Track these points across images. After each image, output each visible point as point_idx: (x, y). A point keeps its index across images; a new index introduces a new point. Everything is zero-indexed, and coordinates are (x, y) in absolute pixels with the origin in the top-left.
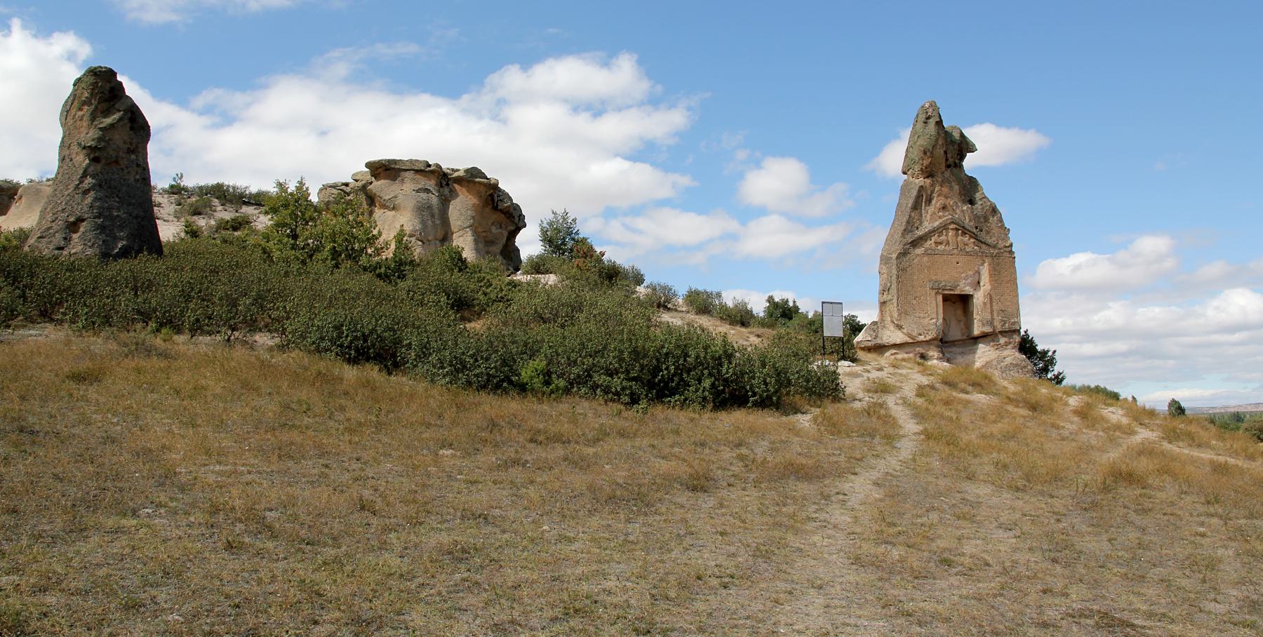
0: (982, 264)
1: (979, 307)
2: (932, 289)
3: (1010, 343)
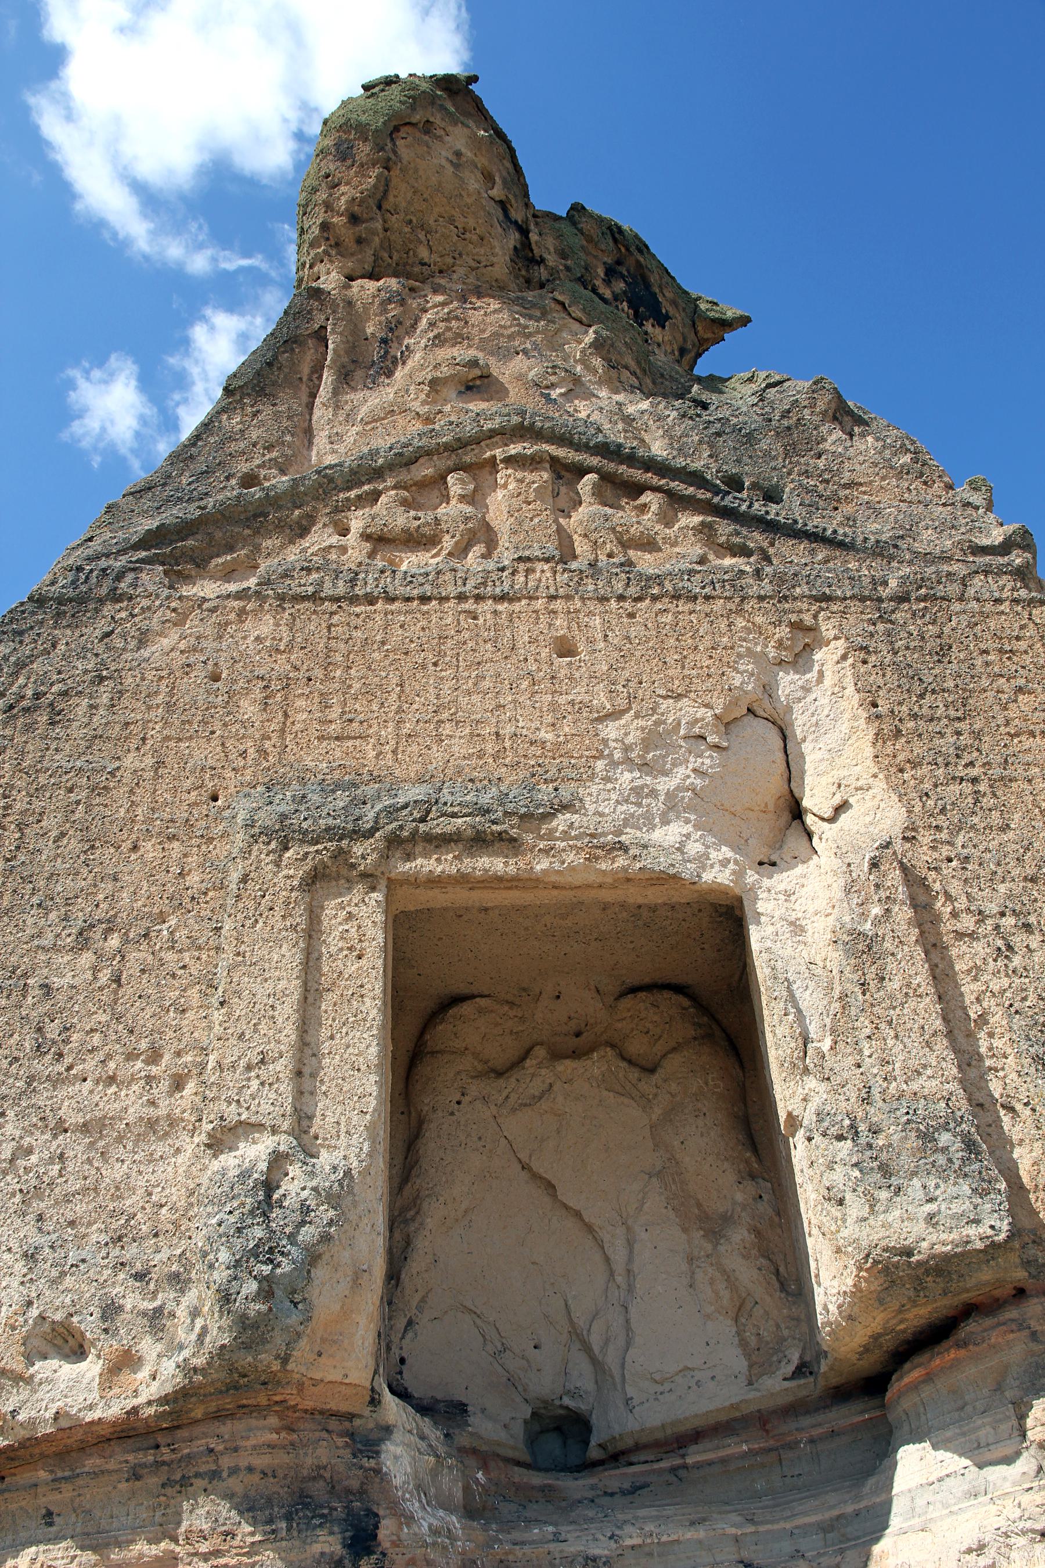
1: (810, 999)
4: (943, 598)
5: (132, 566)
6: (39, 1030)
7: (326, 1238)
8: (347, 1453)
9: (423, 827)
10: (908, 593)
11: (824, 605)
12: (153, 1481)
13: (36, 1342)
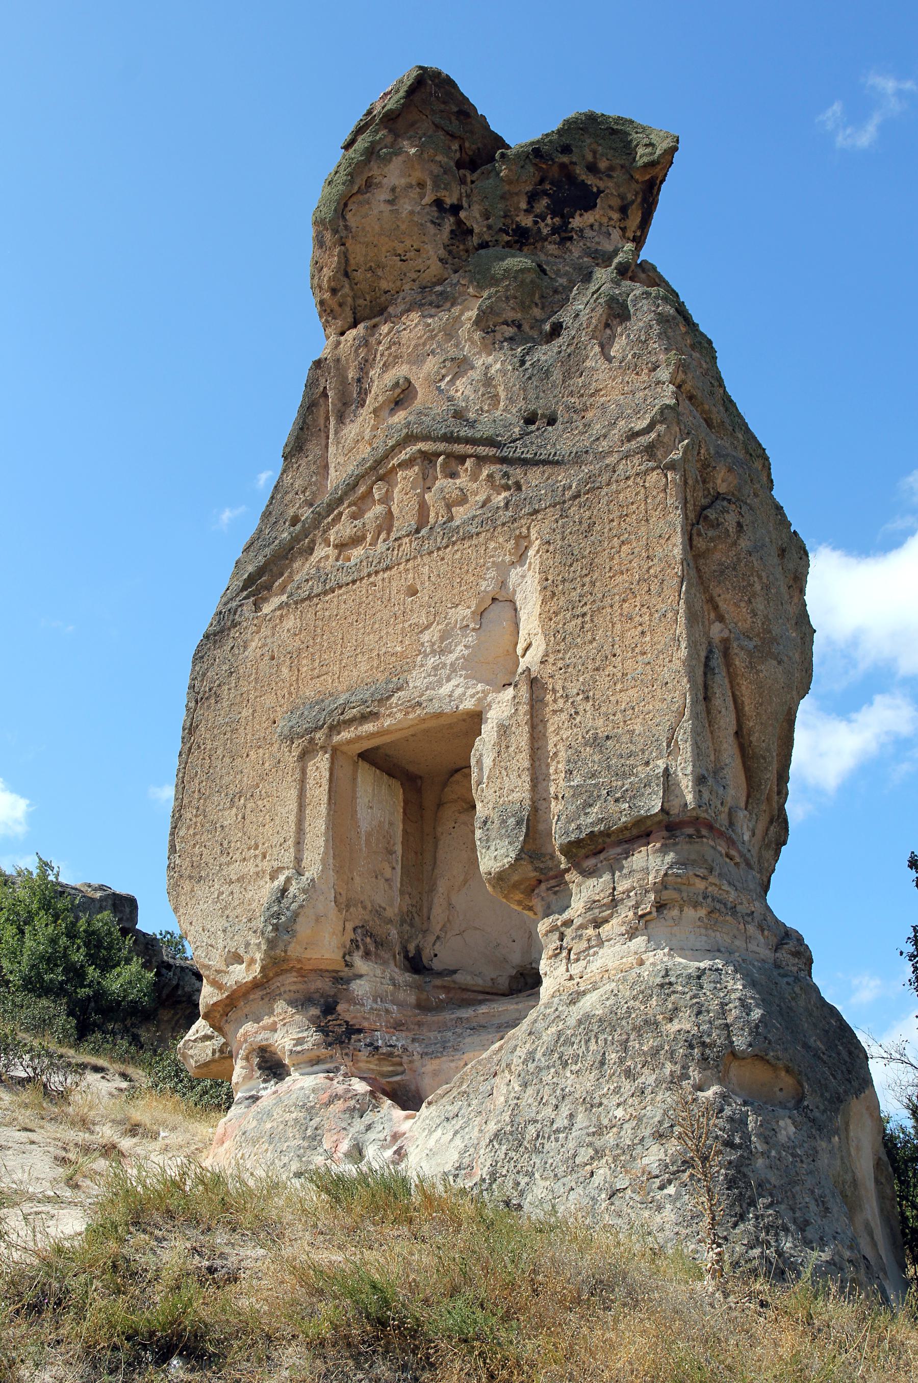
0: (521, 557)
2: (290, 738)
3: (614, 903)
4: (598, 488)
5: (239, 603)
6: (221, 844)
7: (301, 906)
8: (330, 984)
9: (342, 718)
10: (579, 491)
11: (534, 517)
12: (267, 999)
13: (229, 960)
